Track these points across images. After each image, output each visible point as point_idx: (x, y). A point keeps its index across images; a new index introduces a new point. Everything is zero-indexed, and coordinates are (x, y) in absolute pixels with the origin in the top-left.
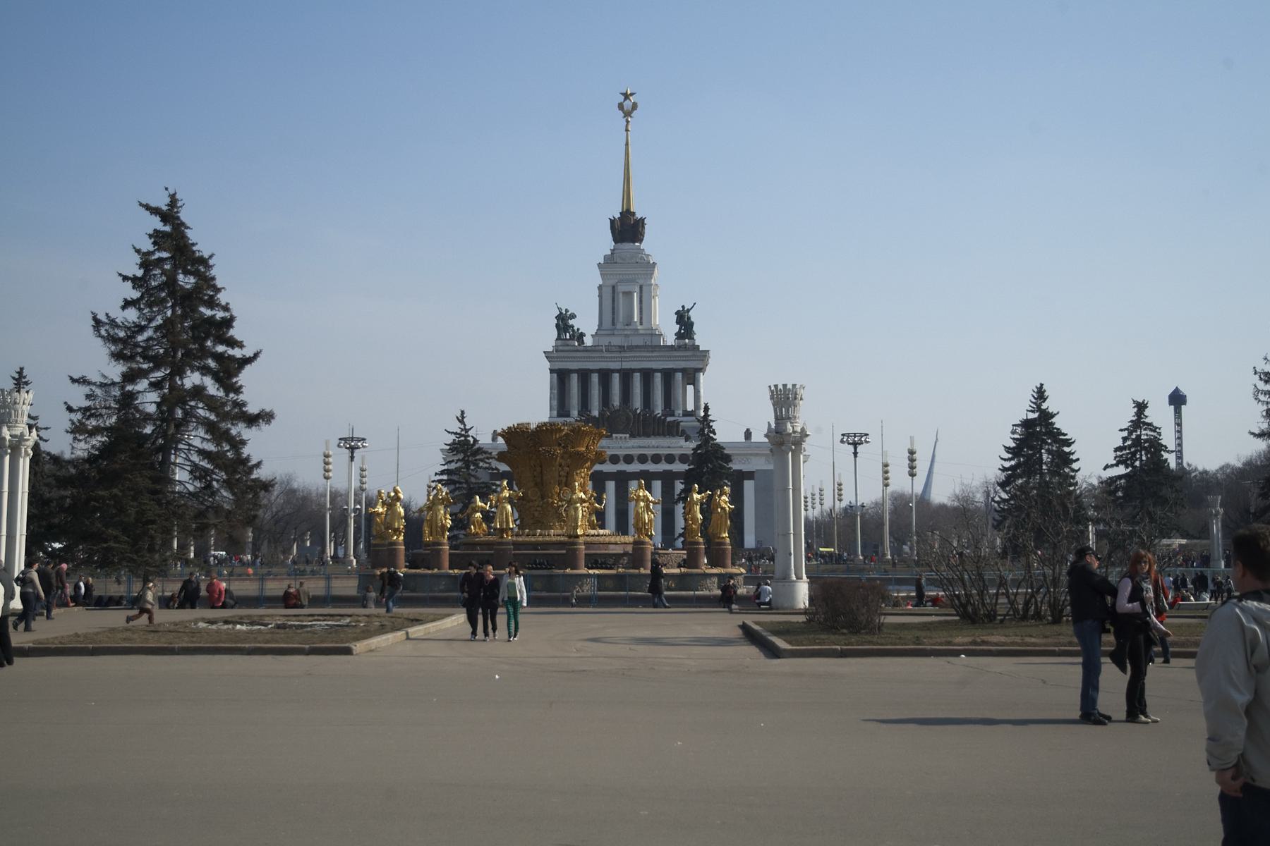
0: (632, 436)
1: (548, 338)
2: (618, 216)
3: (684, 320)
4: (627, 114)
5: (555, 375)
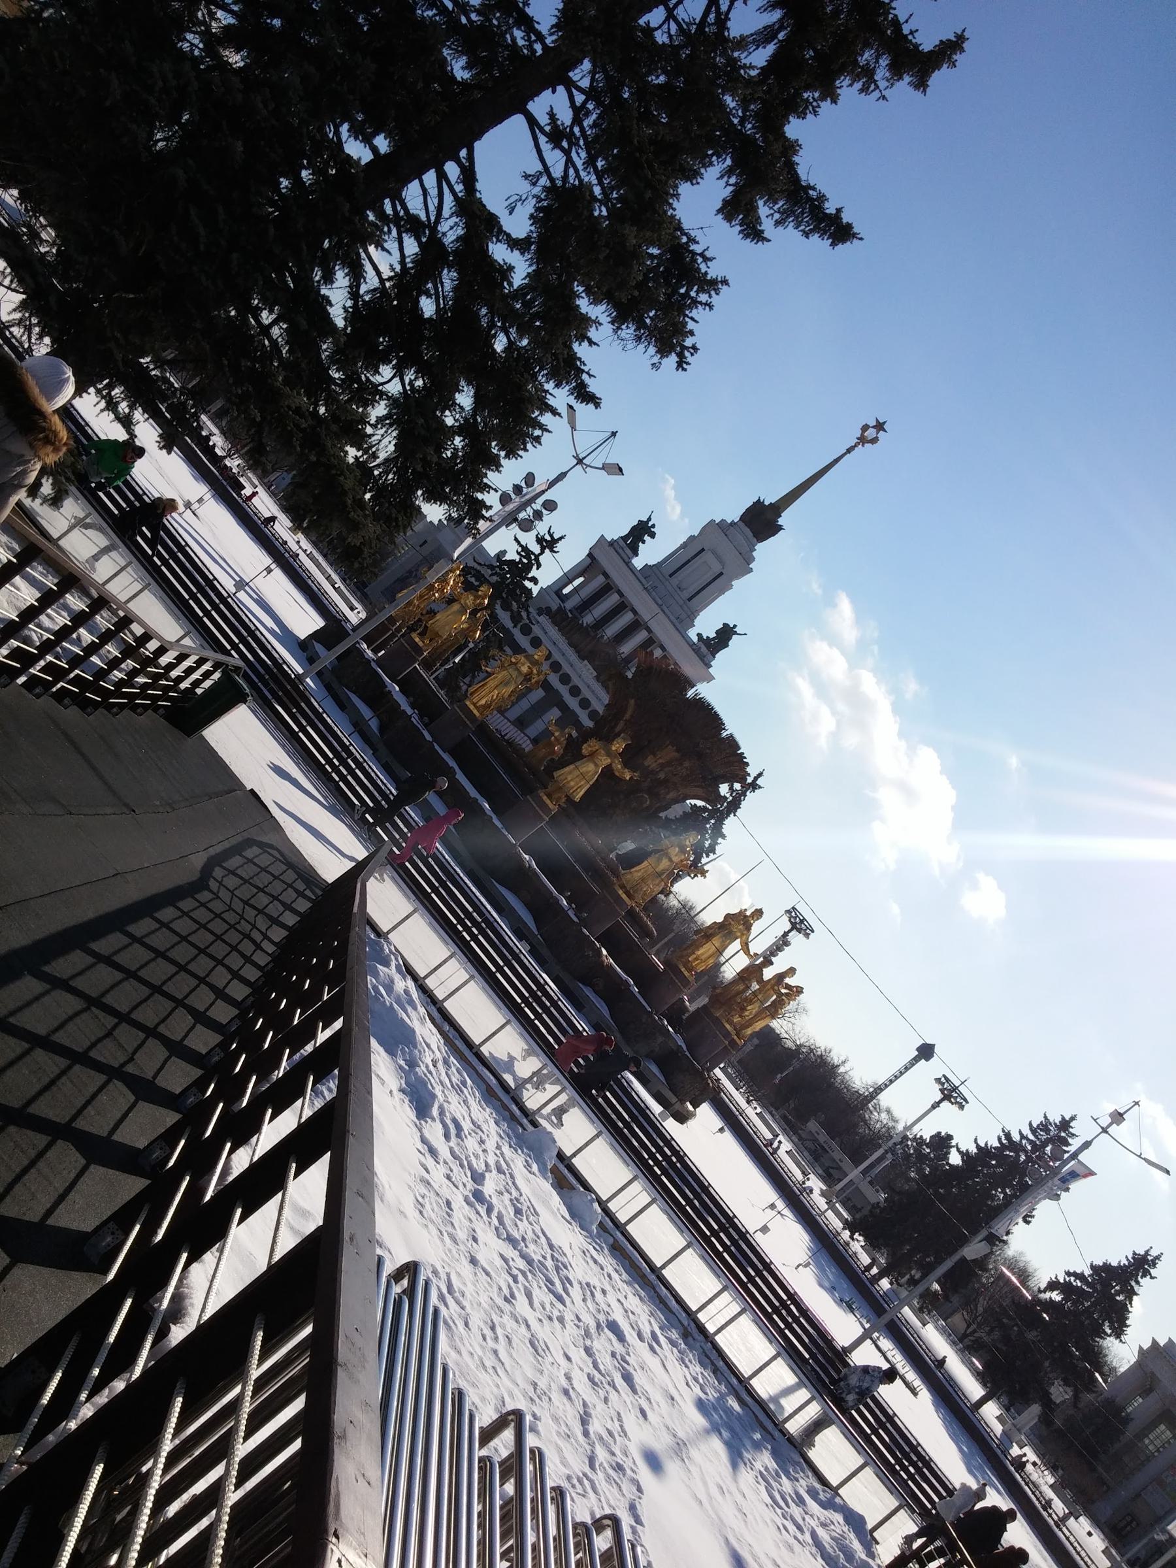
0: (597, 678)
1: (618, 529)
2: (767, 503)
3: (725, 634)
4: (862, 440)
5: (589, 561)
